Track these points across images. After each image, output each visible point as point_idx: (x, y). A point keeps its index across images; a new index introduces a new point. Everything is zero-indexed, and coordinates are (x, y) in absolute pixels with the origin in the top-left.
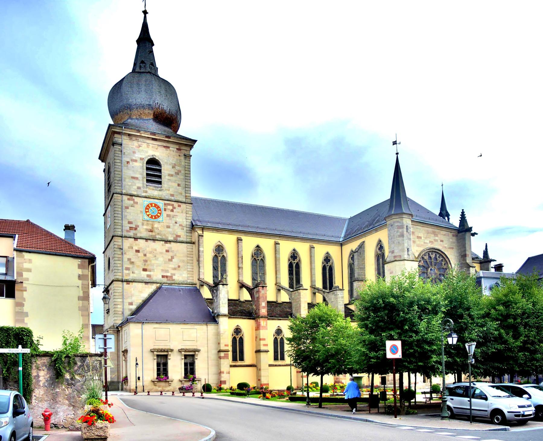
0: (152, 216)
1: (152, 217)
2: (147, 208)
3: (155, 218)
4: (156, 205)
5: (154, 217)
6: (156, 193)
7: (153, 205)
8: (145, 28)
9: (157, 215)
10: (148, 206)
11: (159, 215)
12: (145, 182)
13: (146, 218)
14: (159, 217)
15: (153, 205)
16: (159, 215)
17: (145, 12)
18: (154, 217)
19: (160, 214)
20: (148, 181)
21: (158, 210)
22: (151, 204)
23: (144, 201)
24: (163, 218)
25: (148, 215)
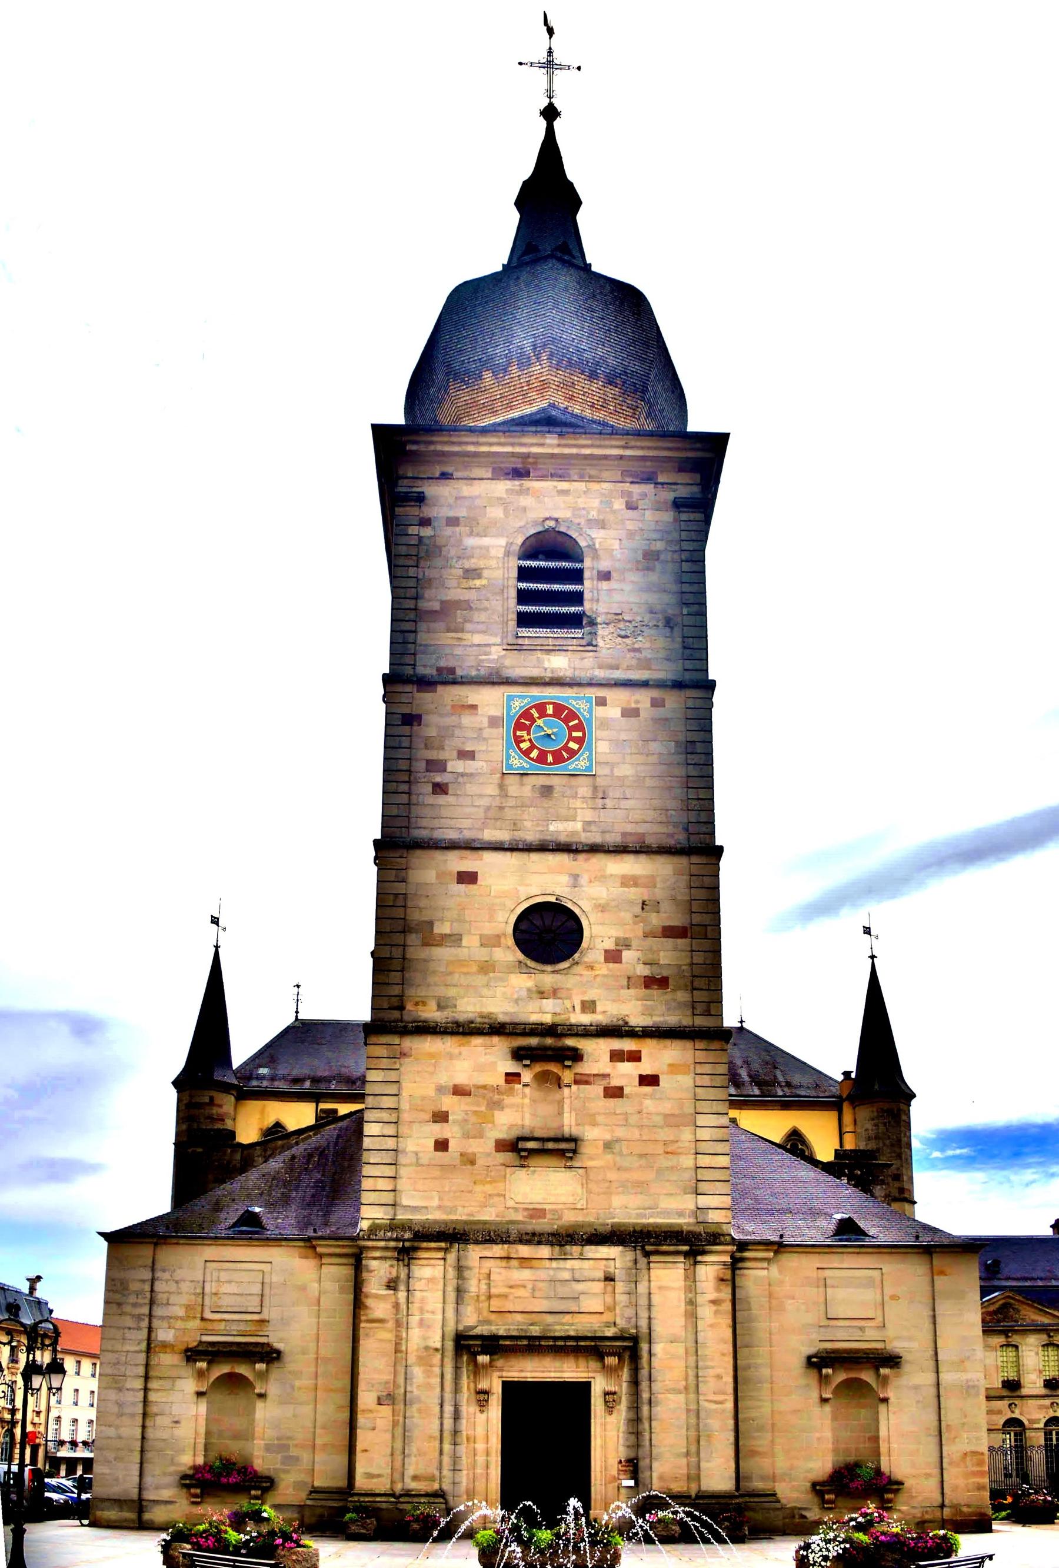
0: (542, 759)
1: (542, 759)
2: (524, 721)
3: (558, 758)
4: (559, 709)
5: (550, 759)
6: (559, 663)
7: (550, 710)
8: (550, 152)
9: (566, 748)
10: (526, 714)
11: (573, 746)
12: (513, 623)
13: (518, 762)
14: (573, 753)
15: (550, 710)
16: (573, 746)
17: (550, 113)
18: (550, 759)
19: (580, 741)
20: (524, 620)
21: (571, 729)
22: (541, 708)
23: (510, 698)
24: (590, 759)
25: (526, 753)
